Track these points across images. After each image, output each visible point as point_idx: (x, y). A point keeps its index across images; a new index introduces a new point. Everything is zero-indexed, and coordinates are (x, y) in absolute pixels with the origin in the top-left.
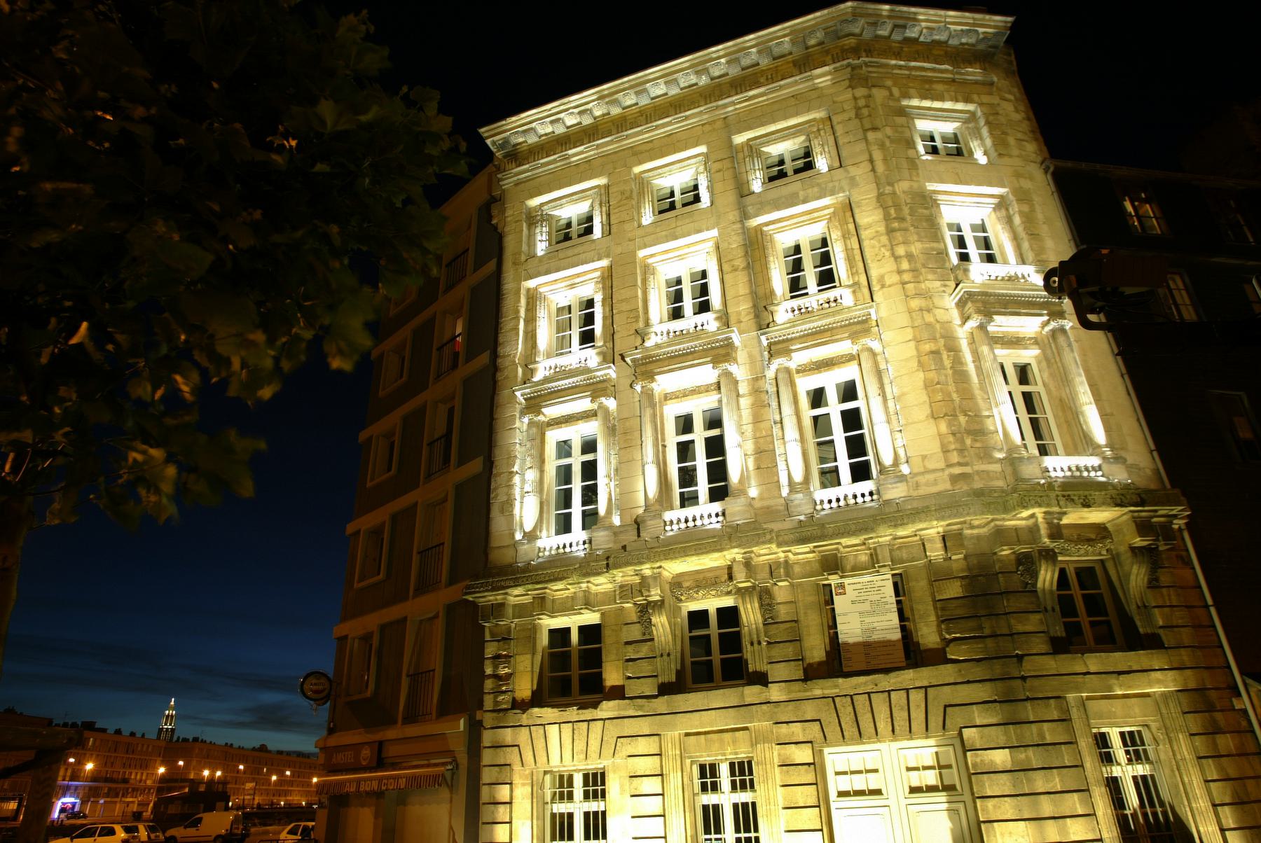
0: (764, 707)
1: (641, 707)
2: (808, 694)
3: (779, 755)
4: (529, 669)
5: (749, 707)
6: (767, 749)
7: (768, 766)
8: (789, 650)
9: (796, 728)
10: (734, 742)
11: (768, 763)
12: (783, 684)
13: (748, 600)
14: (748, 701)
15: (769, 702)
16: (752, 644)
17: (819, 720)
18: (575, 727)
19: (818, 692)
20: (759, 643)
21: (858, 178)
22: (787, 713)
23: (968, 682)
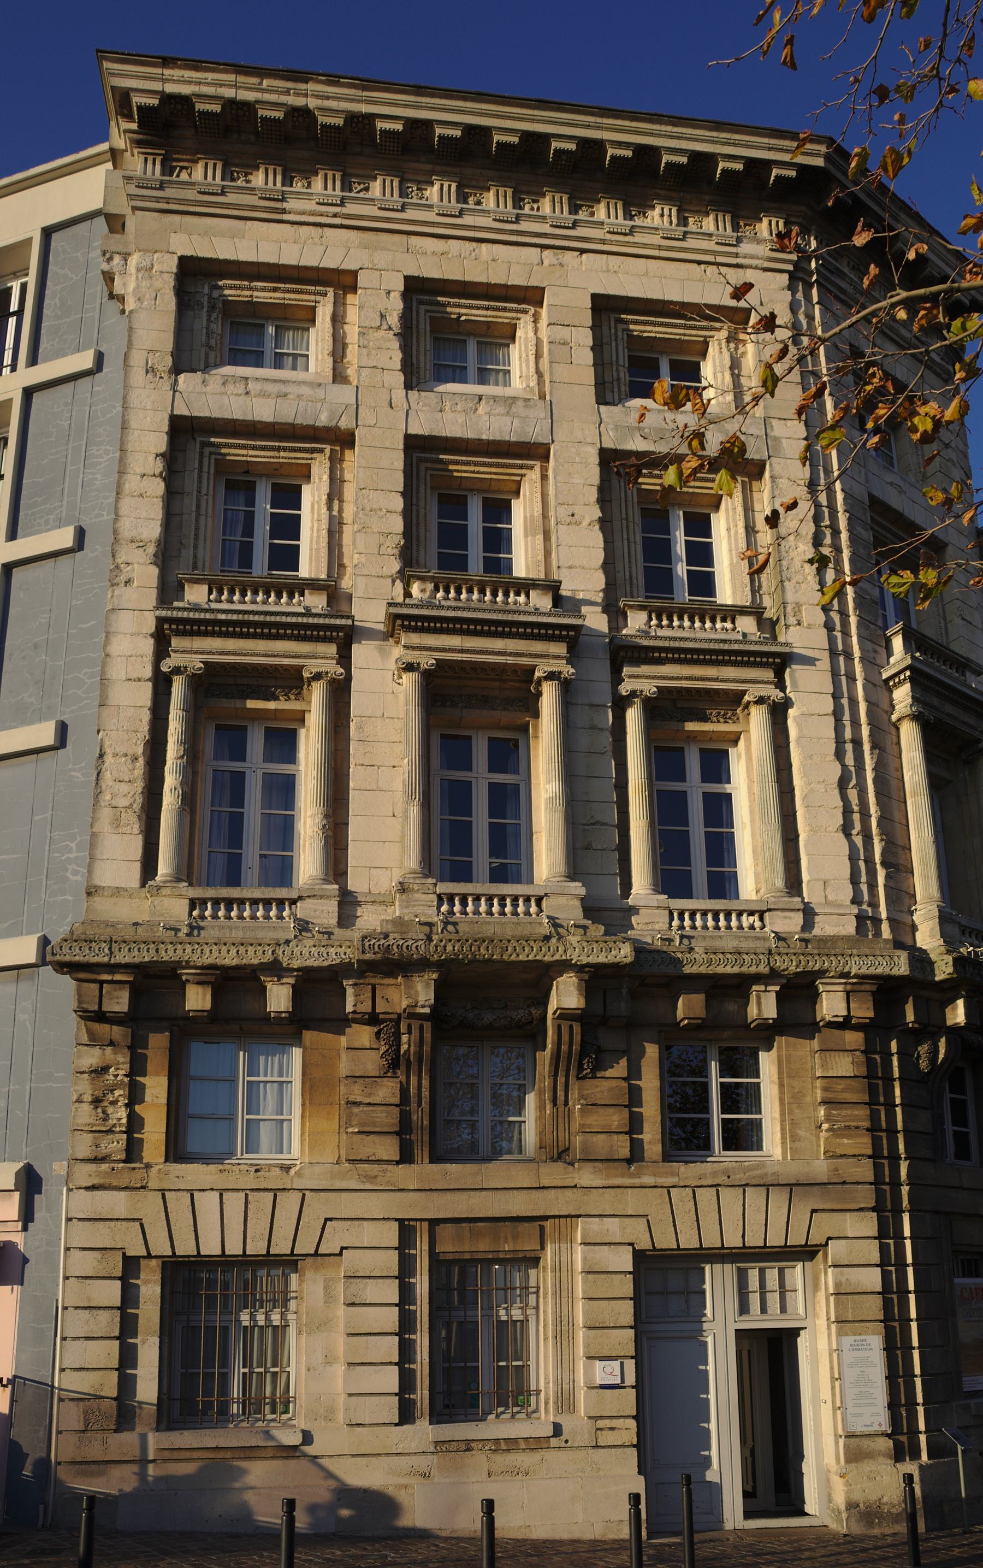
0: (569, 1193)
2: (637, 1181)
7: (564, 1275)
9: (612, 1225)
10: (515, 1237)
11: (564, 1269)
19: (648, 1180)
22: (605, 1201)
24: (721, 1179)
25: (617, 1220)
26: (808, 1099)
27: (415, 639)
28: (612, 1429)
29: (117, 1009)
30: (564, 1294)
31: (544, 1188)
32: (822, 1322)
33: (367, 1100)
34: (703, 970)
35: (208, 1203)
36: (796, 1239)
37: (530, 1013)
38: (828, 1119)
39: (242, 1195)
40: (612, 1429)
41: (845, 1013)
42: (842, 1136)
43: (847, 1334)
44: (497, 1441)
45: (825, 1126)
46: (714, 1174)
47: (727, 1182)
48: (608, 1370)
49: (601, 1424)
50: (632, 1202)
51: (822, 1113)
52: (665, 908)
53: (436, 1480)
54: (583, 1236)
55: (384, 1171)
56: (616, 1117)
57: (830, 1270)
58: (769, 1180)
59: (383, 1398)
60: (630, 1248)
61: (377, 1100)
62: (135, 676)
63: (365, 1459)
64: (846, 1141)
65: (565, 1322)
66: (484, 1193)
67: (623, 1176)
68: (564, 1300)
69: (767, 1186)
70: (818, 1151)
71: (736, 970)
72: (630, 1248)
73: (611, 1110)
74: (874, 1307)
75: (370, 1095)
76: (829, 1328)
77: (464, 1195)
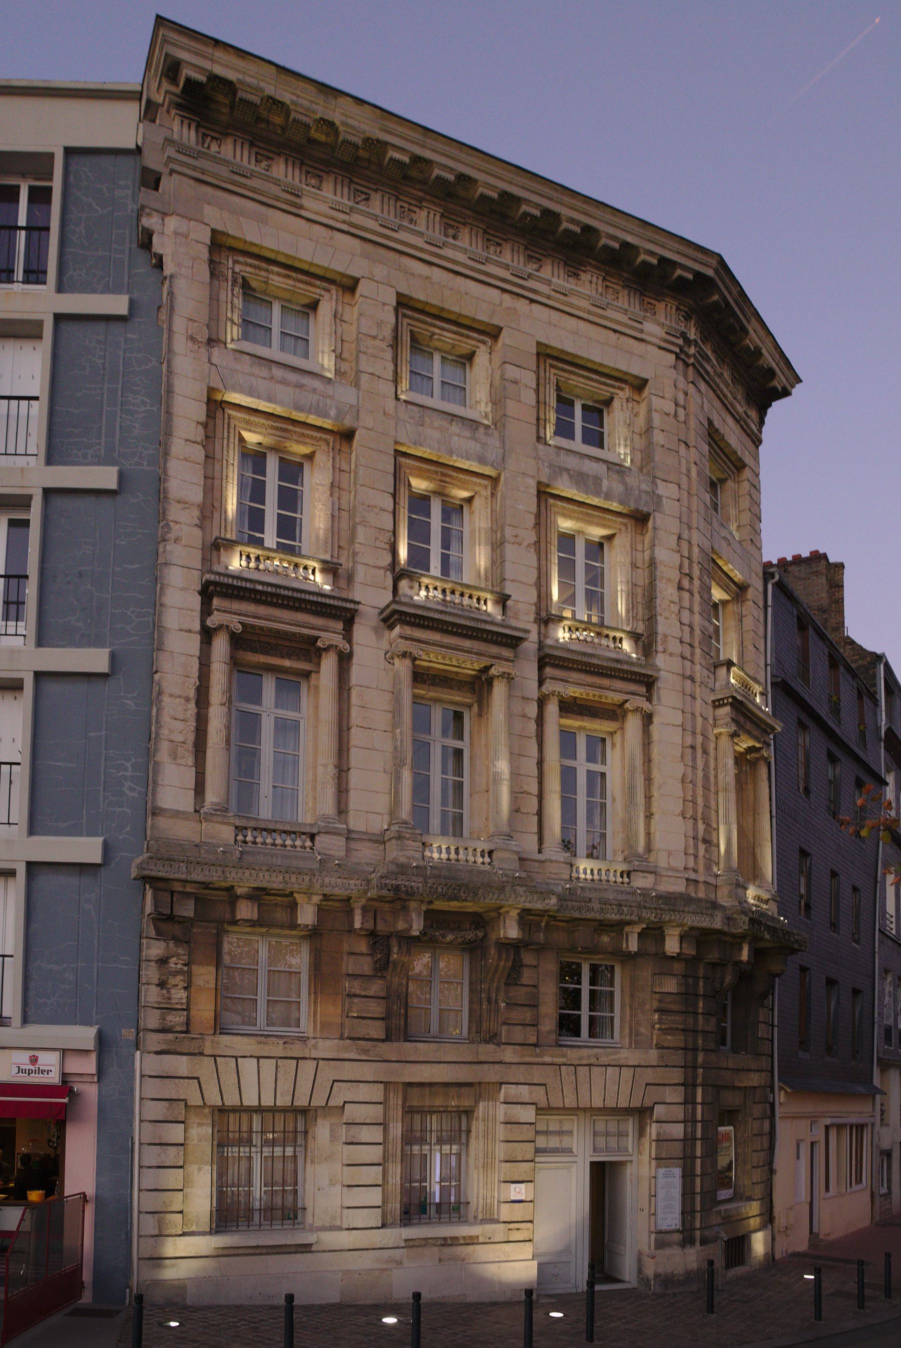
0: (497, 1067)
1: (366, 1051)
3: (506, 1113)
4: (213, 986)
5: (482, 1065)
6: (490, 1106)
7: (490, 1124)
8: (527, 1015)
10: (459, 1096)
11: (490, 1119)
12: (517, 1047)
13: (504, 957)
14: (482, 1058)
15: (501, 1062)
16: (489, 1001)
17: (545, 1085)
18: (279, 1063)
19: (547, 1059)
20: (496, 1001)
21: (664, 499)
22: (520, 1074)
23: (667, 1066)
24: (593, 1061)
25: (527, 1087)
26: (648, 1007)
27: (408, 631)
28: (518, 1229)
29: (185, 914)
30: (490, 1137)
31: (482, 1063)
32: (646, 1158)
33: (363, 993)
34: (598, 916)
35: (249, 1067)
36: (636, 1104)
37: (476, 935)
38: (660, 1021)
39: (274, 1061)
40: (518, 1229)
41: (678, 950)
42: (668, 1034)
43: (661, 1167)
44: (445, 1239)
45: (657, 1026)
46: (589, 1057)
47: (596, 1063)
48: (518, 1190)
49: (512, 1226)
50: (537, 1075)
51: (656, 1017)
52: (568, 863)
53: (405, 1265)
54: (505, 1097)
55: (375, 1046)
56: (529, 1014)
57: (654, 1125)
58: (621, 1062)
59: (371, 1210)
60: (534, 1107)
61: (371, 993)
62: (186, 627)
63: (359, 1252)
64: (669, 1037)
65: (490, 1156)
66: (442, 1065)
67: (532, 1056)
68: (490, 1142)
69: (620, 1066)
70: (652, 1043)
71: (618, 917)
72: (534, 1107)
73: (526, 1009)
74: (677, 1149)
75: (366, 989)
76: (650, 1163)
77: (428, 1066)
